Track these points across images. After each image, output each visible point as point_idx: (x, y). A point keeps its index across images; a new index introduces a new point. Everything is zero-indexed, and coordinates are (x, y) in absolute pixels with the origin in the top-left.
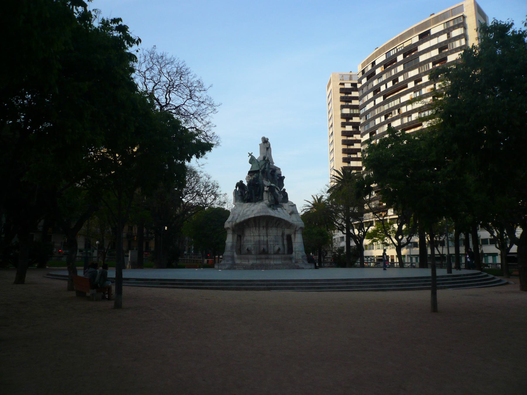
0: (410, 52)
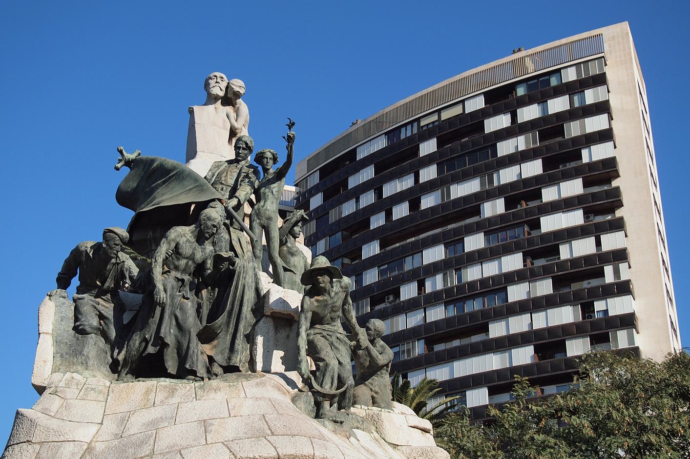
0: (457, 135)
